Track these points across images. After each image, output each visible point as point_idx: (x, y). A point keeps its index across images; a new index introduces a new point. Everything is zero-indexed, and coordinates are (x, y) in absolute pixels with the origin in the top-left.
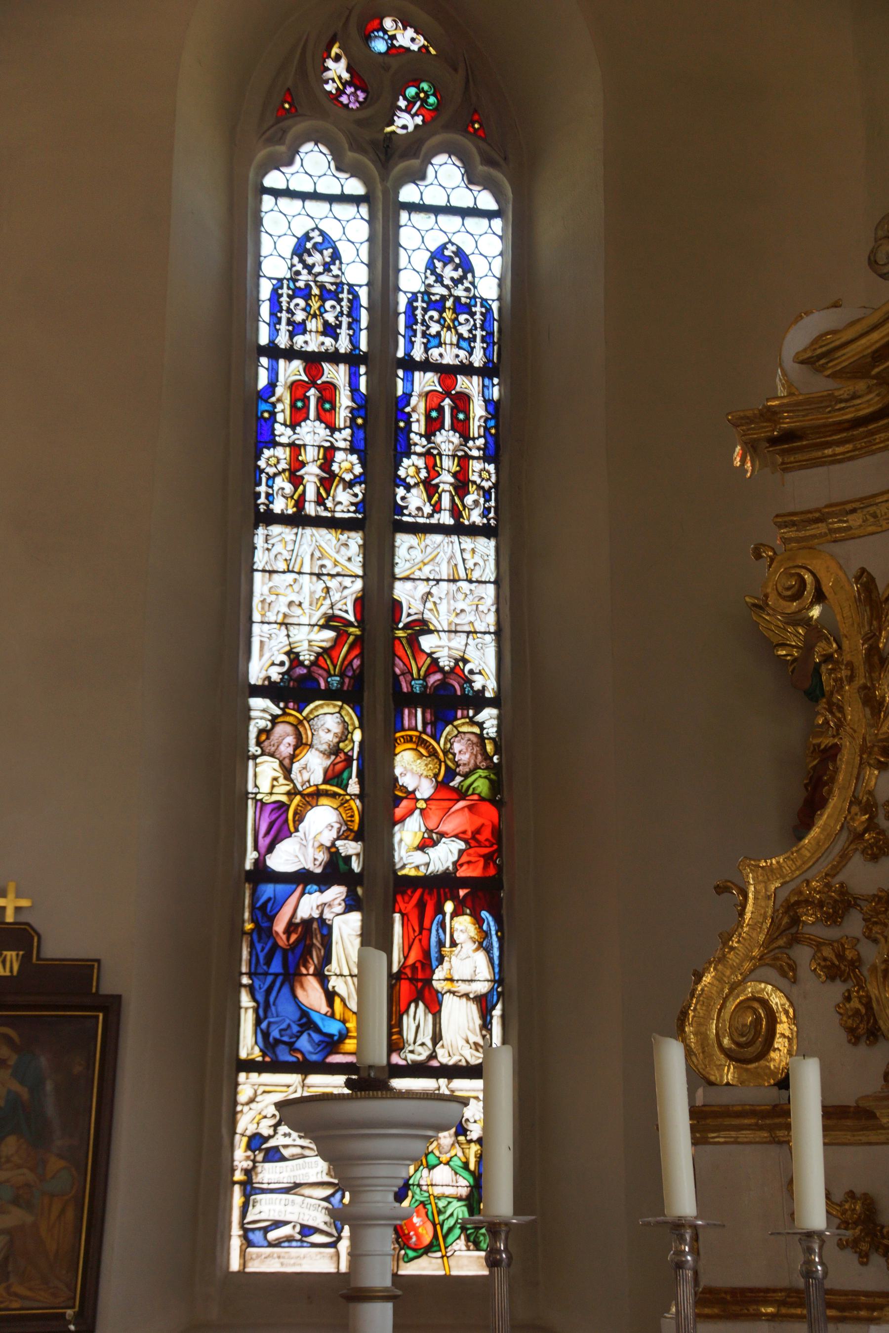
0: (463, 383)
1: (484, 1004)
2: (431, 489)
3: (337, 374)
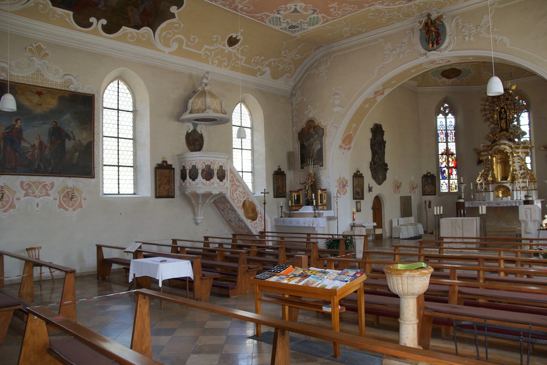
0: (452, 131)
1: (456, 175)
3: (443, 131)
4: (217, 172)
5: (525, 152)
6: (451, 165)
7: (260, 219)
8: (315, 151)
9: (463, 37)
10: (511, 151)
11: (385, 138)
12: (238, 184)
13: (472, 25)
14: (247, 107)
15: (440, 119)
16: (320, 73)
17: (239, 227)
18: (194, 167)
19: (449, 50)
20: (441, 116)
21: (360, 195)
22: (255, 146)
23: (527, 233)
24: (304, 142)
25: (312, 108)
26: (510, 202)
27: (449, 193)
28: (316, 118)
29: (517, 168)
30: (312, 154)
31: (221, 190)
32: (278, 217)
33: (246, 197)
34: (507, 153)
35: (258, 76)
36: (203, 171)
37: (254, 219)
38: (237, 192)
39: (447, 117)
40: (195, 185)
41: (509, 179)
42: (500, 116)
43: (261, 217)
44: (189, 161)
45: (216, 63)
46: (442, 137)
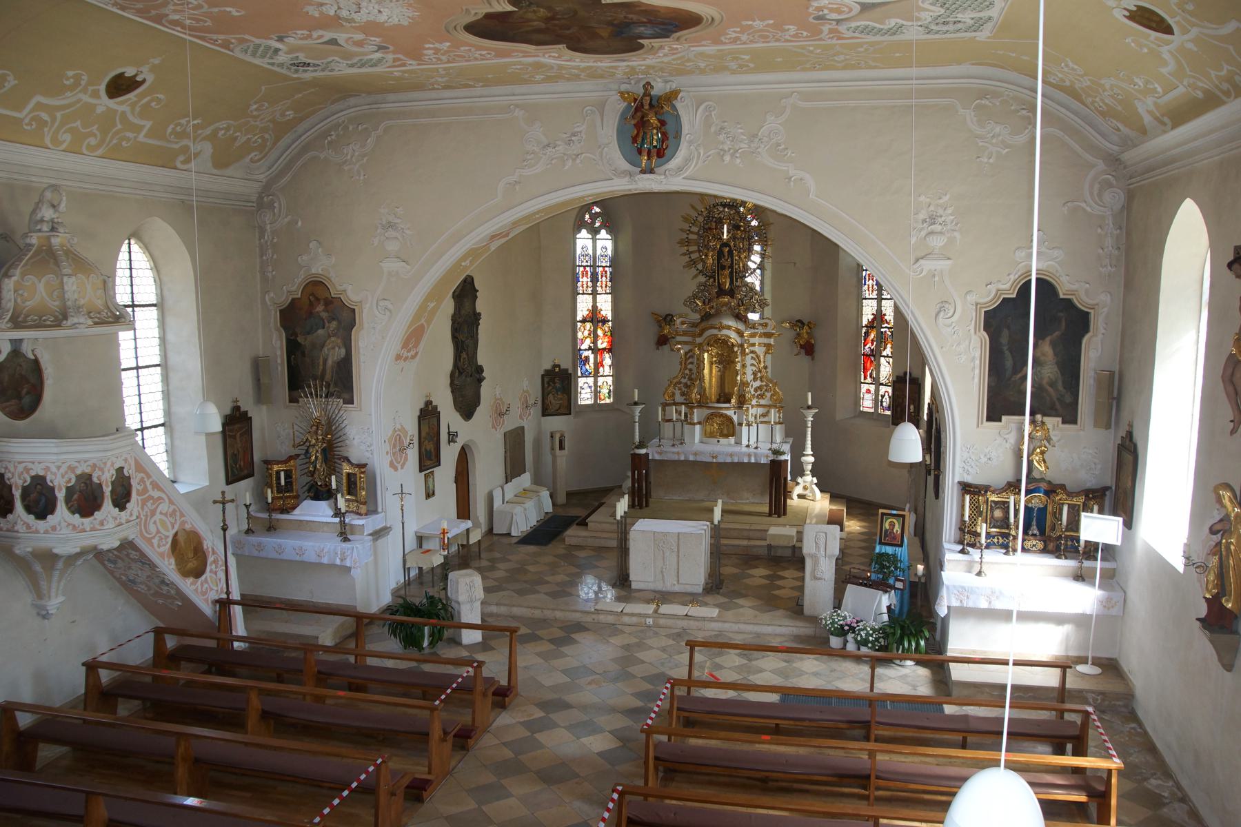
1: (610, 366)
2: (602, 287)
4: (110, 489)
5: (765, 345)
6: (603, 344)
7: (214, 566)
8: (330, 362)
9: (719, 153)
10: (740, 342)
11: (480, 306)
12: (156, 494)
13: (742, 131)
14: (147, 248)
15: (583, 240)
16: (346, 161)
17: (158, 594)
18: (39, 481)
19: (685, 175)
20: (584, 233)
21: (433, 457)
22: (170, 355)
23: (815, 578)
24: (297, 336)
25: (320, 250)
26: (738, 454)
27: (596, 407)
28: (333, 279)
29: (749, 377)
30: (321, 367)
31: (123, 535)
32: (239, 531)
33: (178, 522)
34: (733, 345)
35: (179, 165)
36: (70, 491)
37: (198, 573)
38: (158, 517)
39: (598, 237)
40: (46, 532)
41: (733, 401)
42: (719, 259)
43: (215, 562)
44: (20, 463)
45: (64, 141)
46: (585, 283)
